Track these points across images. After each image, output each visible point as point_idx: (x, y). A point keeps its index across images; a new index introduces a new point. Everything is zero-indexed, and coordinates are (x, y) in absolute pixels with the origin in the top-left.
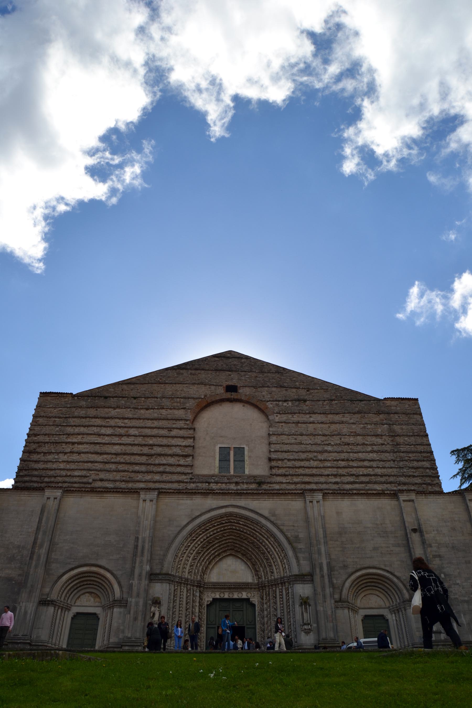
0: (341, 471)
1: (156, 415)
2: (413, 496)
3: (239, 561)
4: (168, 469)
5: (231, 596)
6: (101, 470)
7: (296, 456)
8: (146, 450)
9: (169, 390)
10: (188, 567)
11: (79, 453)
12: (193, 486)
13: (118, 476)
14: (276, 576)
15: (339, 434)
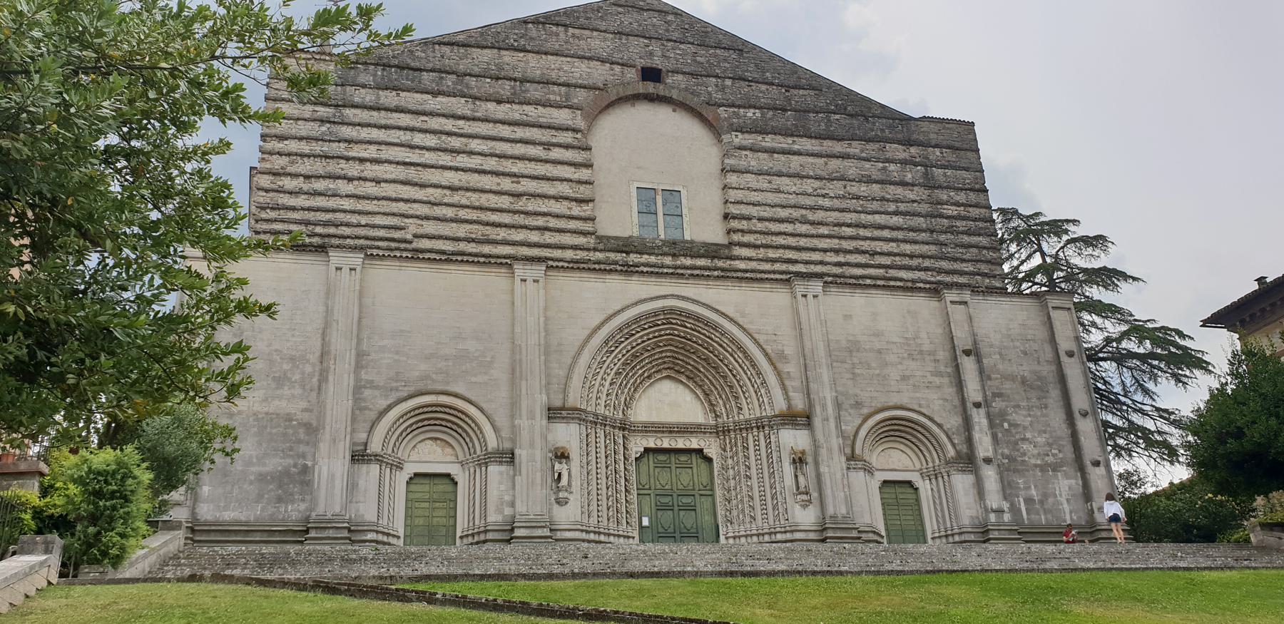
0: (846, 245)
1: (517, 116)
2: (967, 295)
3: (681, 387)
4: (553, 223)
5: (674, 446)
6: (427, 218)
7: (768, 212)
8: (506, 184)
9: (534, 65)
10: (604, 397)
11: (378, 182)
12: (599, 256)
13: (461, 230)
14: (746, 415)
15: (842, 178)
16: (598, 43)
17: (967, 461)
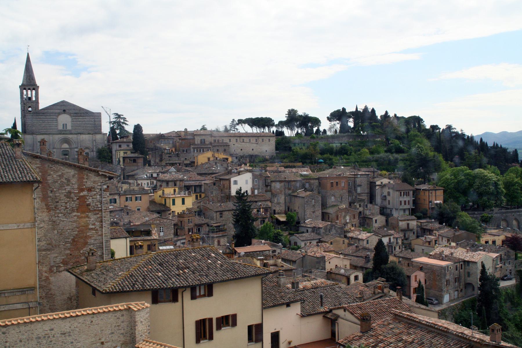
16: (58, 107)
17: (93, 151)
